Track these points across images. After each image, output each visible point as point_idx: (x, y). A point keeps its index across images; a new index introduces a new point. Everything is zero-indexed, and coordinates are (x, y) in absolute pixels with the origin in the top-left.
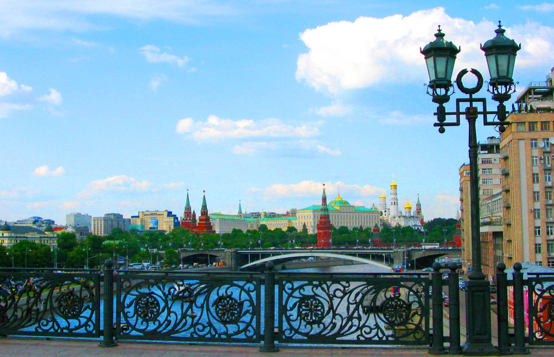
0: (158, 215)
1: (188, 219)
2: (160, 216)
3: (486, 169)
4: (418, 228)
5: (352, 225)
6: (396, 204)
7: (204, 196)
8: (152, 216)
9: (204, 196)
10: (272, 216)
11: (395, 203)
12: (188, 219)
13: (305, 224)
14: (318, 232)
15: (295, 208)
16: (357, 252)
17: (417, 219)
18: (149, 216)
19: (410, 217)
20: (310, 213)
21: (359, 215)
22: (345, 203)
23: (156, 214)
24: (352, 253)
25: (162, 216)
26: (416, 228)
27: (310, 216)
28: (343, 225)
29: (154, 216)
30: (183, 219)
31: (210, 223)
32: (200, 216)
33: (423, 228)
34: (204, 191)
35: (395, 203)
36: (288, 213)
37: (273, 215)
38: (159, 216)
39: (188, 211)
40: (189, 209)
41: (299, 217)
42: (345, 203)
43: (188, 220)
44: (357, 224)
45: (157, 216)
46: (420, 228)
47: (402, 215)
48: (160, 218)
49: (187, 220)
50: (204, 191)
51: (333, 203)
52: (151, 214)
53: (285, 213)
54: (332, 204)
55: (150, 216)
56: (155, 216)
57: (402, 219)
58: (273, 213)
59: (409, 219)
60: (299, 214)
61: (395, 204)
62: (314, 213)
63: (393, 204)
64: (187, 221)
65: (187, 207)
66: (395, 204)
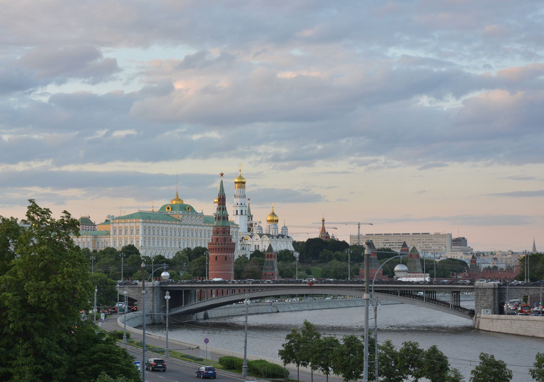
11: (242, 211)
15: (87, 216)
16: (399, 287)
17: (288, 240)
19: (278, 237)
20: (137, 224)
22: (189, 208)
24: (390, 289)
27: (138, 230)
35: (242, 211)
41: (115, 231)
42: (189, 208)
47: (262, 232)
51: (168, 208)
54: (167, 209)
57: (265, 239)
59: (277, 239)
60: (115, 225)
61: (242, 214)
62: (145, 224)
63: (239, 213)
66: (242, 214)
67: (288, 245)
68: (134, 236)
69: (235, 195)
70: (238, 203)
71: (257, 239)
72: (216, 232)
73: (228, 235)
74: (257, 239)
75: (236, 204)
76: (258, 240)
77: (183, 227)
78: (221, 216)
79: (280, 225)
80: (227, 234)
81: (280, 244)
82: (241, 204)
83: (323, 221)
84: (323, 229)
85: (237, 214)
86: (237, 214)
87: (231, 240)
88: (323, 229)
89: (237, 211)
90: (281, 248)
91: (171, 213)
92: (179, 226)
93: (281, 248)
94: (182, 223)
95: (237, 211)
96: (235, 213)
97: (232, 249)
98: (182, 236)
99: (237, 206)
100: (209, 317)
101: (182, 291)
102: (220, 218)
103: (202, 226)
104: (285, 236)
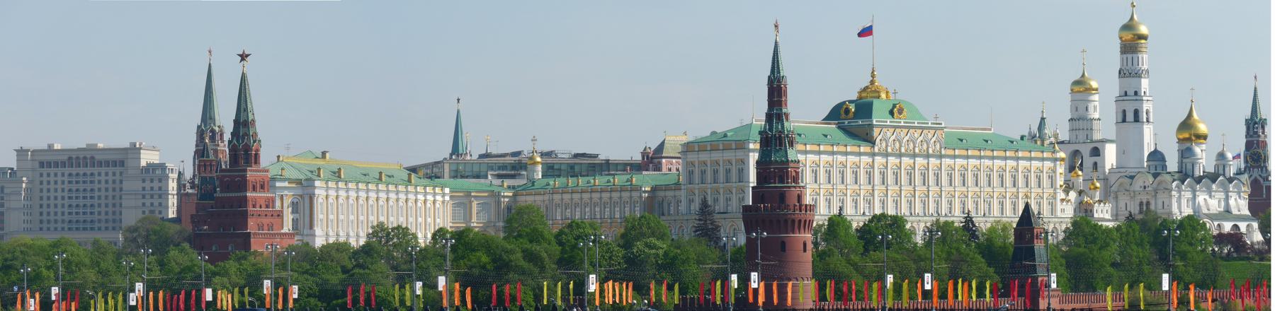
2: (111, 170)
4: (1236, 227)
5: (918, 208)
8: (74, 171)
10: (577, 169)
13: (704, 204)
14: (750, 241)
18: (59, 170)
23: (92, 158)
25: (118, 170)
26: (1227, 227)
28: (878, 211)
29: (81, 170)
33: (1255, 225)
34: (243, 57)
35: (1137, 113)
37: (587, 165)
38: (103, 170)
40: (218, 137)
45: (96, 170)
46: (1243, 226)
47: (1164, 167)
48: (52, 179)
50: (243, 57)
52: (70, 158)
53: (638, 157)
55: (67, 170)
56: (89, 170)
58: (584, 155)
63: (1130, 117)
67: (1232, 202)
69: (1120, 73)
70: (1126, 92)
71: (1145, 187)
73: (793, 184)
74: (1145, 187)
75: (1123, 94)
76: (1147, 189)
77: (879, 160)
78: (772, 137)
80: (788, 183)
81: (1207, 197)
82: (1136, 93)
85: (1124, 120)
86: (1124, 120)
87: (799, 198)
90: (1209, 210)
91: (851, 122)
93: (1209, 210)
94: (876, 150)
95: (1124, 111)
96: (1120, 120)
97: (805, 221)
98: (876, 183)
99: (1125, 98)
102: (772, 141)
103: (941, 157)
104: (1221, 178)
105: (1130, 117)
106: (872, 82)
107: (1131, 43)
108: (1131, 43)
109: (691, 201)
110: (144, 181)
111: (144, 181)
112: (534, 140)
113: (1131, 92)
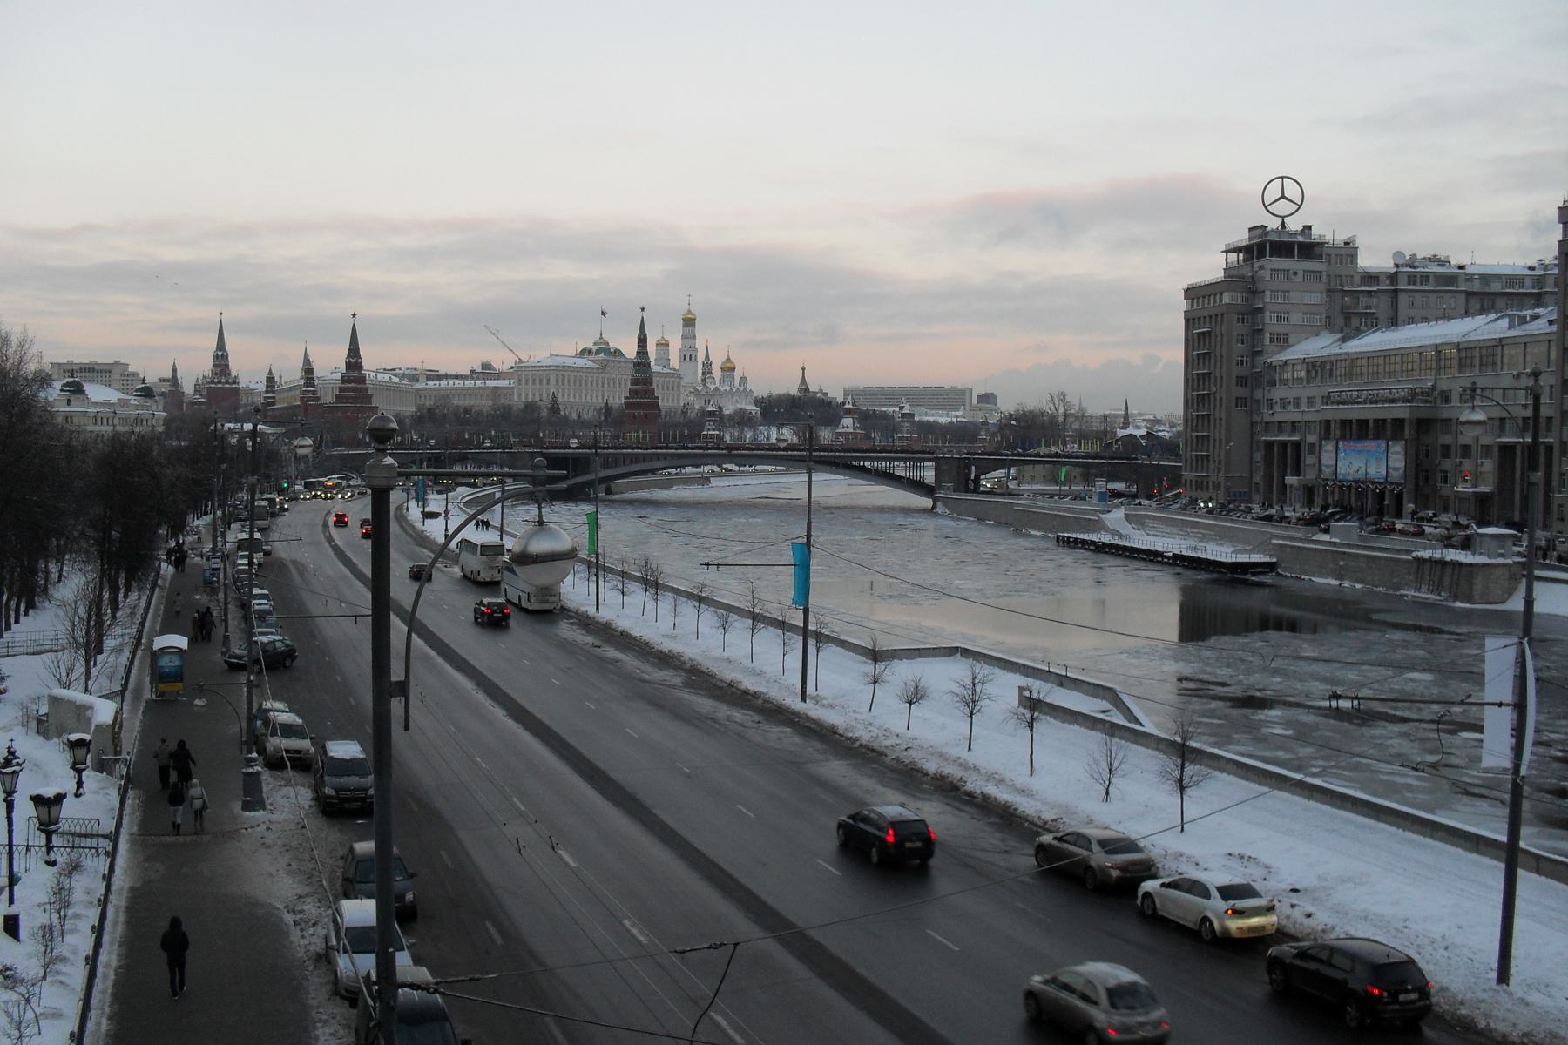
0: (97, 372)
1: (223, 380)
2: (104, 374)
3: (1278, 292)
6: (693, 358)
7: (354, 326)
9: (354, 326)
11: (691, 356)
12: (223, 380)
21: (668, 382)
23: (93, 369)
25: (108, 375)
27: (548, 380)
30: (212, 382)
31: (367, 390)
32: (344, 371)
35: (691, 356)
36: (473, 371)
39: (223, 363)
43: (223, 384)
44: (600, 398)
45: (96, 374)
49: (219, 382)
52: (81, 369)
61: (690, 359)
63: (688, 358)
64: (220, 385)
65: (220, 353)
68: (537, 385)
72: (634, 382)
79: (737, 374)
83: (803, 369)
84: (803, 381)
87: (653, 394)
88: (803, 381)
89: (685, 356)
92: (603, 375)
95: (685, 356)
100: (613, 491)
101: (569, 459)
105: (688, 358)
106: (601, 338)
107: (689, 322)
108: (689, 322)
109: (548, 394)
110: (123, 380)
111: (123, 380)
112: (423, 362)
113: (688, 347)
